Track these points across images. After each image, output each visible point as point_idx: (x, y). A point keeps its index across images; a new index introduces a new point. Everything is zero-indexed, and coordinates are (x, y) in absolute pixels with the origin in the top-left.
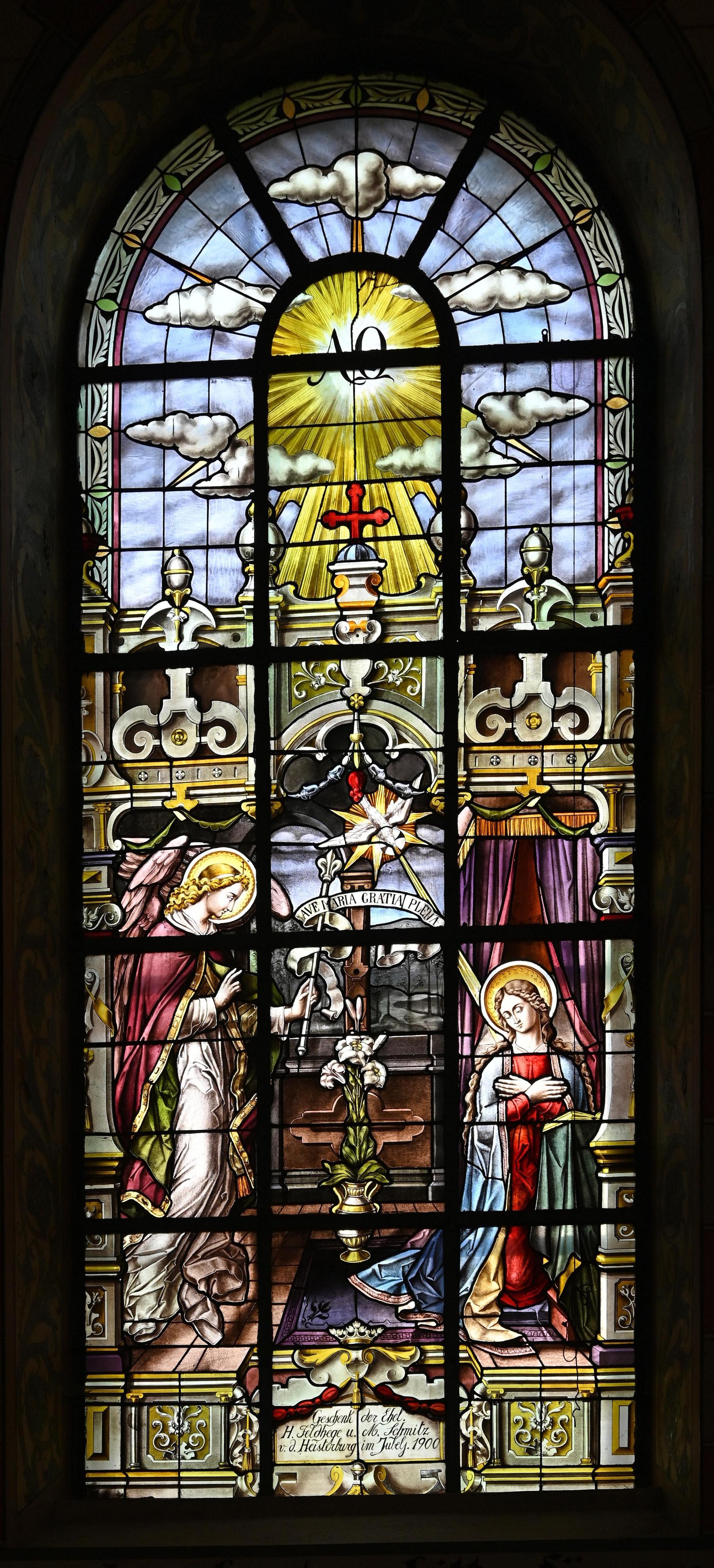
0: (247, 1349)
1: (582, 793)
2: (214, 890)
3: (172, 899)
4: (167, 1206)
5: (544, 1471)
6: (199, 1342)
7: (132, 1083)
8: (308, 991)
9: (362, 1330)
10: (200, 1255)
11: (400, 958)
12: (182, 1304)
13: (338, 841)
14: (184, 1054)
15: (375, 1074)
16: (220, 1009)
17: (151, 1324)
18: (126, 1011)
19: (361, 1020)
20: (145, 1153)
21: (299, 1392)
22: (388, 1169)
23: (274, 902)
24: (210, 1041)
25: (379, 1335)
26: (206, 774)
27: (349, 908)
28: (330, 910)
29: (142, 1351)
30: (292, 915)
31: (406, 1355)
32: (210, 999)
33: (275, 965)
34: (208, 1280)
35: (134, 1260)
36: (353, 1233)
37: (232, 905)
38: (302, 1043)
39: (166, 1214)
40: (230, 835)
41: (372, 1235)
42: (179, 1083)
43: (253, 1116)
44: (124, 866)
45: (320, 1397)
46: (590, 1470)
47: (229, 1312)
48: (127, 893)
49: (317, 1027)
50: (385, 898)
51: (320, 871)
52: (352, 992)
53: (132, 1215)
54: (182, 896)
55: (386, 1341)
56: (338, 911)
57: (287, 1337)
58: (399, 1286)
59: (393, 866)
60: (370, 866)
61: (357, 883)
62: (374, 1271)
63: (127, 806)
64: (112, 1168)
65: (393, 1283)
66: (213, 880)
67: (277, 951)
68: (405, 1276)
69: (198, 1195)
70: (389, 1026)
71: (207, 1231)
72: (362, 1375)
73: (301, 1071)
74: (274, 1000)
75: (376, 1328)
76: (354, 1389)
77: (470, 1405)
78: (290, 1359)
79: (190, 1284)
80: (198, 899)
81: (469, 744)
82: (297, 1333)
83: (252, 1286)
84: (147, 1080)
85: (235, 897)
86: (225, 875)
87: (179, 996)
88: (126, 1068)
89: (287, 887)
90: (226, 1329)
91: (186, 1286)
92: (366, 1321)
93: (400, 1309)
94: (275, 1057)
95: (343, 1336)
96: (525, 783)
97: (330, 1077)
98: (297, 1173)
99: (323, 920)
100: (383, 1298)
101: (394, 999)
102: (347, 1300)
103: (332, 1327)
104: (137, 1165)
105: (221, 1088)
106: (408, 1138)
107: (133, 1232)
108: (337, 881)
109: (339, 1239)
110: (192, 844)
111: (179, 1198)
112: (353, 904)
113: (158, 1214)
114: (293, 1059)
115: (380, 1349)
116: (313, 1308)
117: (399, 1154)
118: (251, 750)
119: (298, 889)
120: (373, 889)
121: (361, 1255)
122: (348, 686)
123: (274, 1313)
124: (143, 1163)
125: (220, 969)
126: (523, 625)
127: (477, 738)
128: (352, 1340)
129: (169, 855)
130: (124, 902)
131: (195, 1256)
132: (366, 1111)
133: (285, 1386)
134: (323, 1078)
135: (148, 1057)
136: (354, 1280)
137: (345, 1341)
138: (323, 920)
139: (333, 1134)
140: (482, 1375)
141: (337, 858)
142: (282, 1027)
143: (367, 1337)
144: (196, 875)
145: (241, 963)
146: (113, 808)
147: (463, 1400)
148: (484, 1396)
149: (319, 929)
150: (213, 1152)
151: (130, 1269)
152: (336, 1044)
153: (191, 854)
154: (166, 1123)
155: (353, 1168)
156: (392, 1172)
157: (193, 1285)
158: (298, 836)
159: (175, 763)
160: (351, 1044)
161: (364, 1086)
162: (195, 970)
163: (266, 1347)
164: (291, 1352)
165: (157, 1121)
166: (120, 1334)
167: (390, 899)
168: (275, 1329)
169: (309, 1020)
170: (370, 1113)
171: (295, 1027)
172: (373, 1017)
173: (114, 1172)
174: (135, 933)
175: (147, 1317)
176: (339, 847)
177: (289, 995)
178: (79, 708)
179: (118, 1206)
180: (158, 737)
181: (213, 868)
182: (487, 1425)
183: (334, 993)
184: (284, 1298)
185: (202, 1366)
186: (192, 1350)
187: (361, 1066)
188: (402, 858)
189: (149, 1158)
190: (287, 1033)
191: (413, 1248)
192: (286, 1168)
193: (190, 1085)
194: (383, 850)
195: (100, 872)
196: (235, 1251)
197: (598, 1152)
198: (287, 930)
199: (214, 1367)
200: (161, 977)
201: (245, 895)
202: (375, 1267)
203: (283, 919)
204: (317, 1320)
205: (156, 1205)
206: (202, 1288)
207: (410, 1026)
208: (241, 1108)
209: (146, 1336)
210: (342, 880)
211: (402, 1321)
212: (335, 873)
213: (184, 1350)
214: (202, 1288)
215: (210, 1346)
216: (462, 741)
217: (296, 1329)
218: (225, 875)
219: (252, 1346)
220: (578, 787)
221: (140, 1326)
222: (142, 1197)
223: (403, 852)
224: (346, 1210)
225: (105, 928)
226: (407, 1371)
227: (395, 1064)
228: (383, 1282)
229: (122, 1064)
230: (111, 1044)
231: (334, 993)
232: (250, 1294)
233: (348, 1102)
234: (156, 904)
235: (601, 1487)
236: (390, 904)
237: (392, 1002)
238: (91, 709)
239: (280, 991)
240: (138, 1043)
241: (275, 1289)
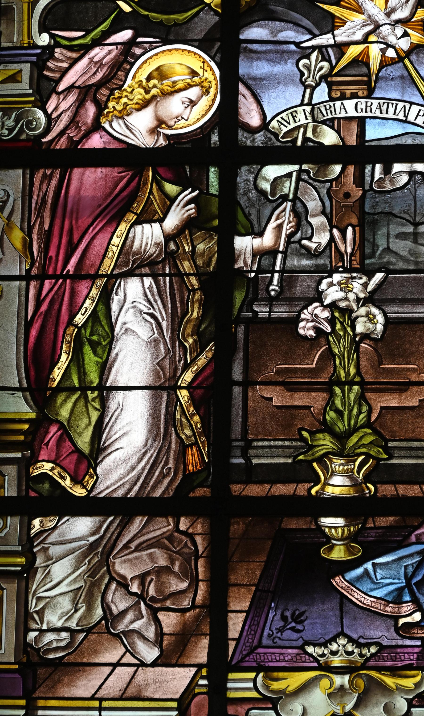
0: (193, 670)
2: (165, 94)
3: (111, 104)
4: (92, 482)
6: (128, 659)
7: (51, 326)
8: (285, 218)
9: (350, 648)
10: (133, 546)
11: (405, 178)
12: (106, 608)
13: (325, 39)
14: (121, 292)
15: (370, 321)
16: (168, 238)
17: (64, 635)
18: (46, 238)
19: (352, 254)
20: (64, 413)
22: (387, 441)
23: (242, 110)
24: (155, 276)
25: (373, 655)
27: (339, 119)
28: (314, 120)
29: (50, 670)
30: (265, 125)
31: (409, 683)
32: (156, 226)
33: (242, 185)
34: (142, 578)
35: (45, 550)
36: (339, 521)
37: (190, 112)
38: (275, 281)
39: (90, 492)
40: (188, 30)
41: (364, 524)
42: (112, 328)
43: (209, 371)
44: (51, 64)
47: (169, 621)
48: (54, 96)
49: (294, 262)
50: (384, 108)
51: (302, 74)
52: (341, 220)
53: (45, 493)
54: (124, 100)
55: (382, 664)
56: (324, 122)
57: (248, 655)
58: (400, 591)
59: (395, 71)
60: (365, 70)
61: (349, 90)
62: (366, 571)
65: (391, 588)
66: (165, 82)
67: (244, 169)
68: (408, 579)
69: (133, 468)
70: (389, 263)
71: (143, 515)
72: (348, 708)
73: (273, 315)
74: (240, 228)
75: (368, 645)
79: (119, 583)
80: (143, 105)
82: (261, 650)
83: (202, 586)
84: (70, 322)
85: (192, 103)
86: (181, 77)
87: (117, 219)
88: (44, 308)
89: (260, 92)
90: (165, 643)
91: (114, 586)
92: (355, 636)
93: (402, 621)
94: (239, 297)
95: (323, 655)
97: (311, 324)
98: (266, 443)
99: (305, 133)
100: (379, 607)
101: (395, 229)
102: (331, 608)
103: (308, 643)
104: (53, 429)
105: (167, 335)
106: (414, 402)
107: (45, 514)
108: (324, 86)
109: (320, 529)
110: (140, 40)
111: (108, 472)
112: (343, 114)
113: (79, 492)
114: (263, 300)
115: (373, 674)
116: (284, 618)
117: (401, 422)
119: (274, 95)
120: (369, 96)
121: (349, 550)
123: (230, 623)
124: (62, 426)
125: (171, 189)
129: (110, 52)
130: (50, 107)
131: (126, 546)
132: (358, 366)
134: (302, 324)
135: (73, 294)
136: (339, 582)
137: (326, 663)
138: (305, 133)
139: (313, 394)
141: (323, 59)
142: (249, 261)
143: (355, 657)
144: (143, 76)
145: (197, 182)
149: (299, 143)
150: (154, 415)
151: (39, 561)
152: (319, 283)
153: (138, 51)
154: (94, 378)
155: (341, 438)
156: (390, 444)
157: (123, 584)
158: (274, 33)
160: (339, 283)
161: (355, 336)
162: (138, 190)
163: (219, 668)
164: (252, 675)
165: (82, 373)
166: (23, 647)
167: (391, 109)
168: (232, 645)
169: (284, 253)
170: (363, 369)
171: (266, 261)
172: (368, 251)
173: (22, 438)
174: (63, 143)
175: (59, 624)
176: (326, 47)
177: (259, 222)
179: (27, 480)
181: (164, 69)
183: (318, 221)
184: (245, 605)
185: (131, 692)
186: (119, 670)
187: (352, 311)
188: (407, 61)
189: (69, 420)
190: (255, 268)
191: (419, 542)
192: (250, 436)
193: (127, 330)
194: (383, 51)
195: (21, 71)
196: (181, 541)
198: (258, 143)
199: (148, 694)
200: (93, 197)
201: (205, 101)
202: (369, 566)
203: (253, 131)
204: (288, 634)
205: (77, 480)
206: (135, 588)
207: (416, 263)
208: (193, 360)
209: (57, 649)
210: (330, 85)
211: (403, 637)
212: (321, 78)
213: (108, 669)
214: (135, 588)
215: (143, 664)
217: (260, 645)
218: (181, 77)
219: (200, 666)
221: (50, 637)
222: (58, 469)
223: (408, 53)
224: (330, 491)
225: (23, 137)
226: (410, 704)
227: (396, 309)
228: (379, 586)
229: (39, 303)
230: (26, 278)
231: (318, 221)
232: (199, 598)
233: (334, 355)
234: (91, 110)
236: (391, 115)
237: (392, 233)
239: (247, 216)
240: (61, 276)
241: (233, 592)
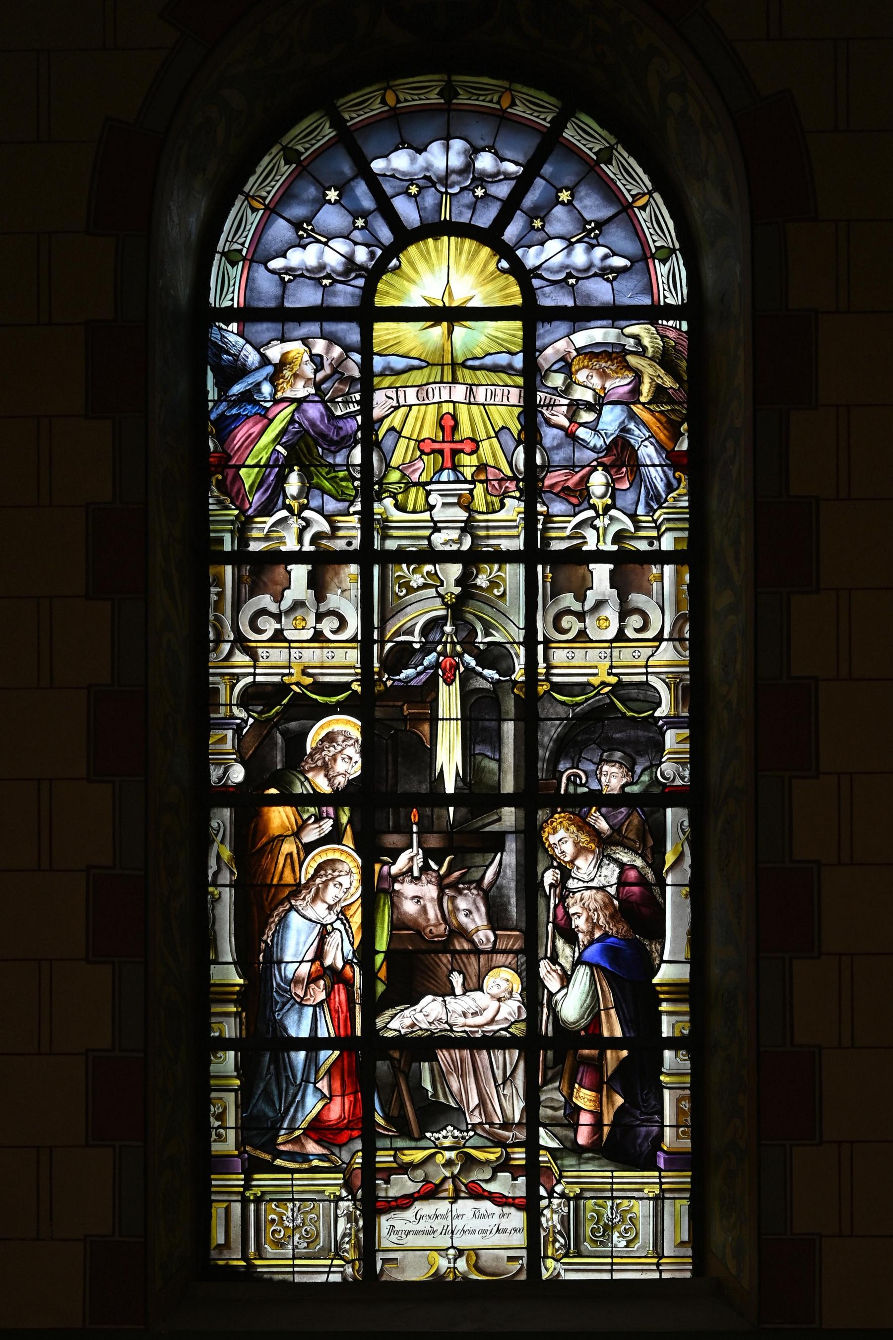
1: (647, 683)
5: (615, 1260)
21: (402, 1185)
45: (418, 1192)
46: (655, 1261)
63: (250, 679)
64: (233, 993)
76: (449, 1185)
77: (550, 1202)
78: (392, 1159)
96: (596, 675)
122: (442, 585)
126: (591, 546)
128: (447, 1143)
137: (441, 1144)
140: (561, 1177)
147: (544, 1198)
148: (563, 1195)
159: (292, 645)
178: (209, 592)
180: (279, 621)
182: (564, 1221)
197: (658, 988)
220: (643, 678)
235: (665, 1276)
238: (221, 595)
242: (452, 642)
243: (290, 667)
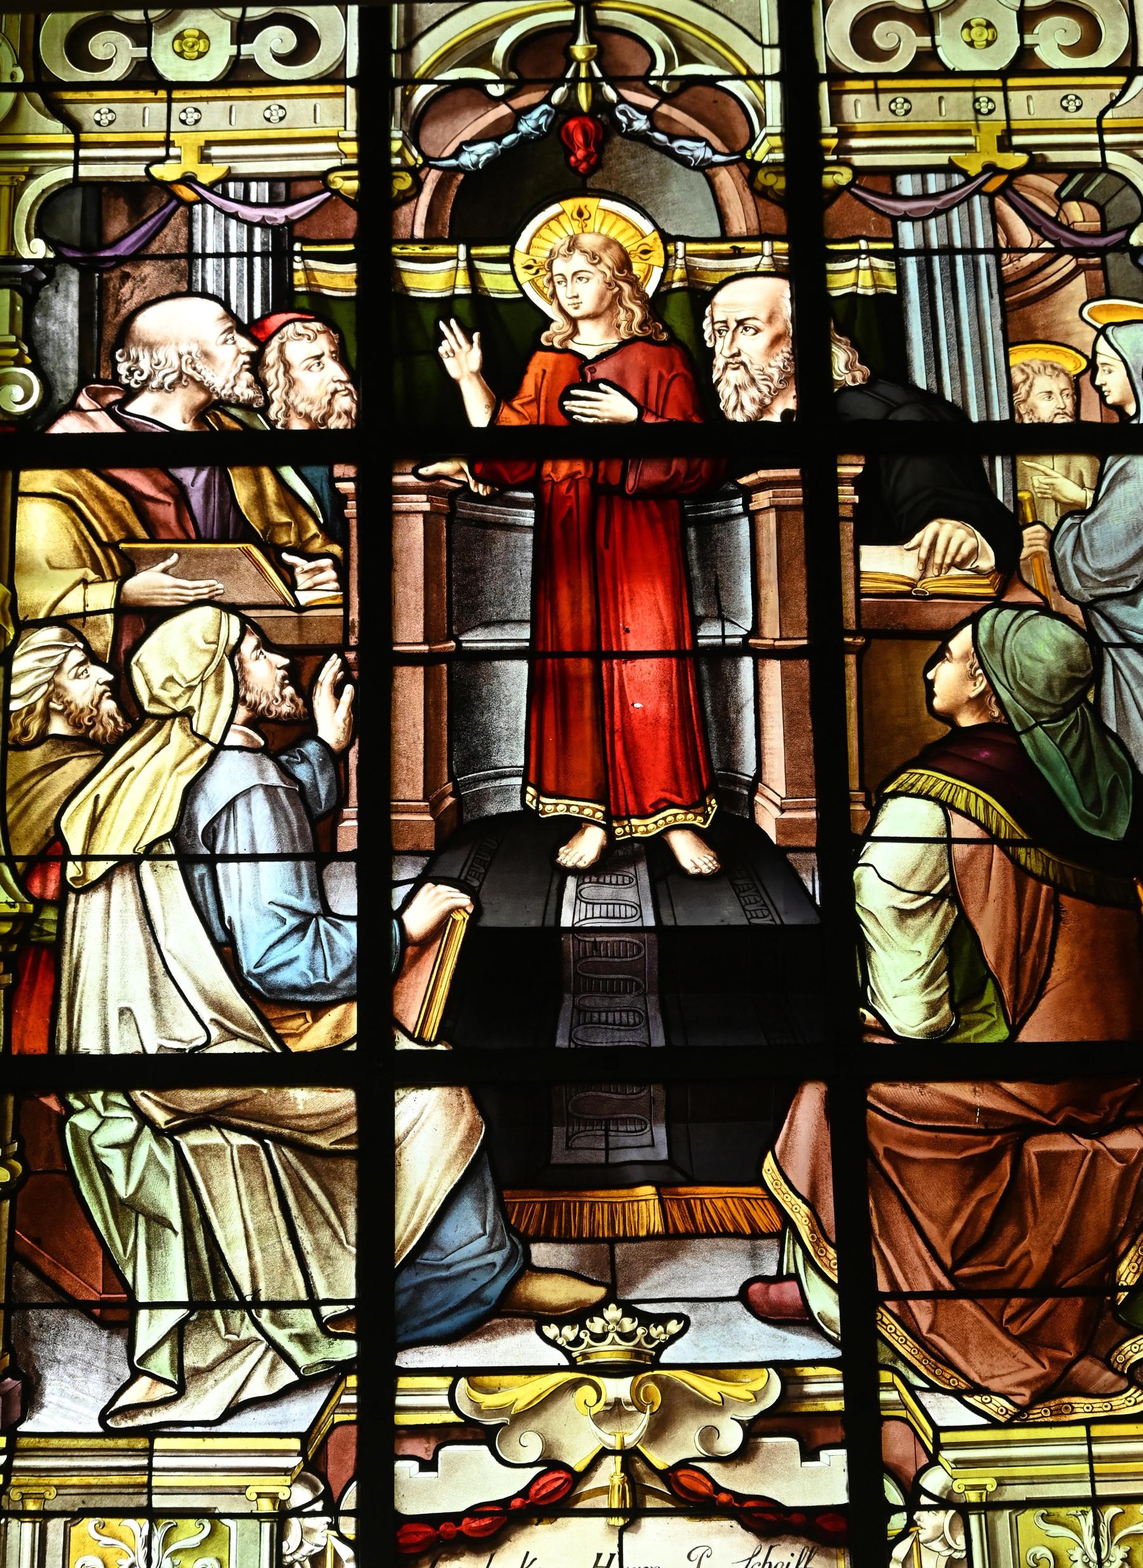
9: (628, 1325)
26: (248, 114)
45: (524, 1493)
63: (67, 173)
76: (610, 1472)
77: (911, 1523)
81: (838, 75)
118: (352, 71)
127: (852, 62)
128: (608, 1352)
133: (429, 1465)
140: (939, 1446)
146: (31, 176)
148: (943, 1503)
159: (176, 94)
216: (823, 69)
242: (591, 79)
243: (168, 143)
